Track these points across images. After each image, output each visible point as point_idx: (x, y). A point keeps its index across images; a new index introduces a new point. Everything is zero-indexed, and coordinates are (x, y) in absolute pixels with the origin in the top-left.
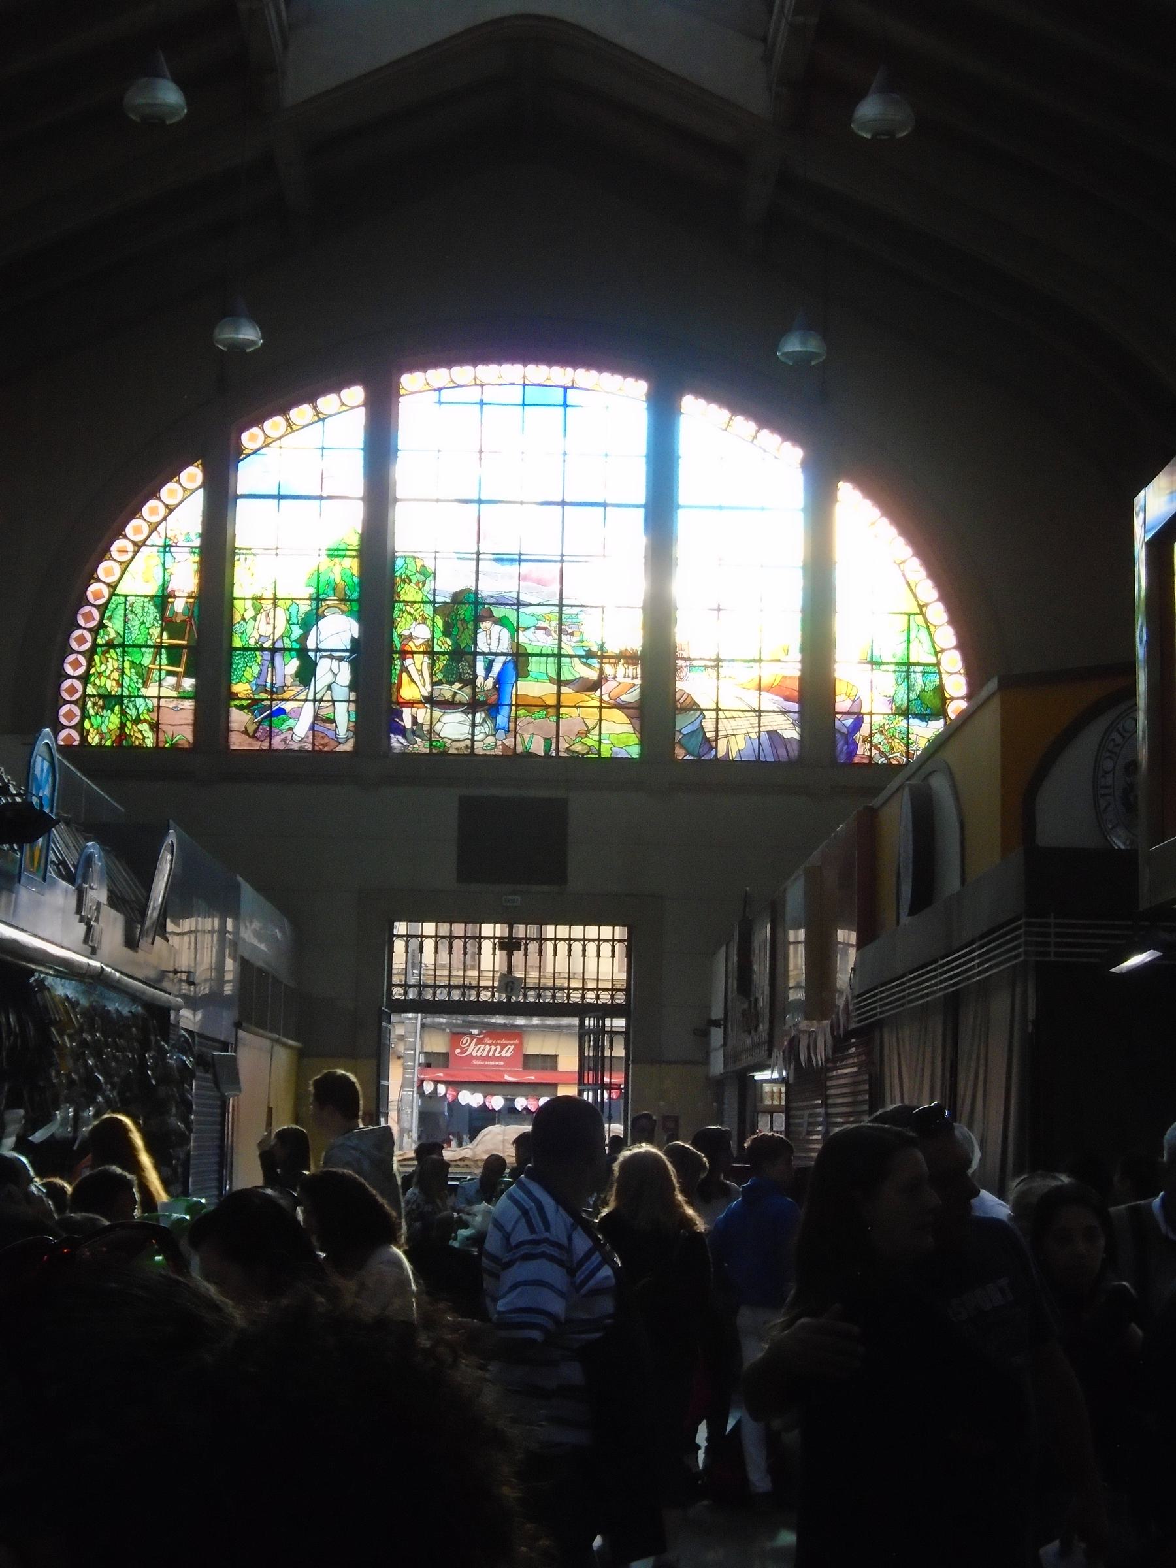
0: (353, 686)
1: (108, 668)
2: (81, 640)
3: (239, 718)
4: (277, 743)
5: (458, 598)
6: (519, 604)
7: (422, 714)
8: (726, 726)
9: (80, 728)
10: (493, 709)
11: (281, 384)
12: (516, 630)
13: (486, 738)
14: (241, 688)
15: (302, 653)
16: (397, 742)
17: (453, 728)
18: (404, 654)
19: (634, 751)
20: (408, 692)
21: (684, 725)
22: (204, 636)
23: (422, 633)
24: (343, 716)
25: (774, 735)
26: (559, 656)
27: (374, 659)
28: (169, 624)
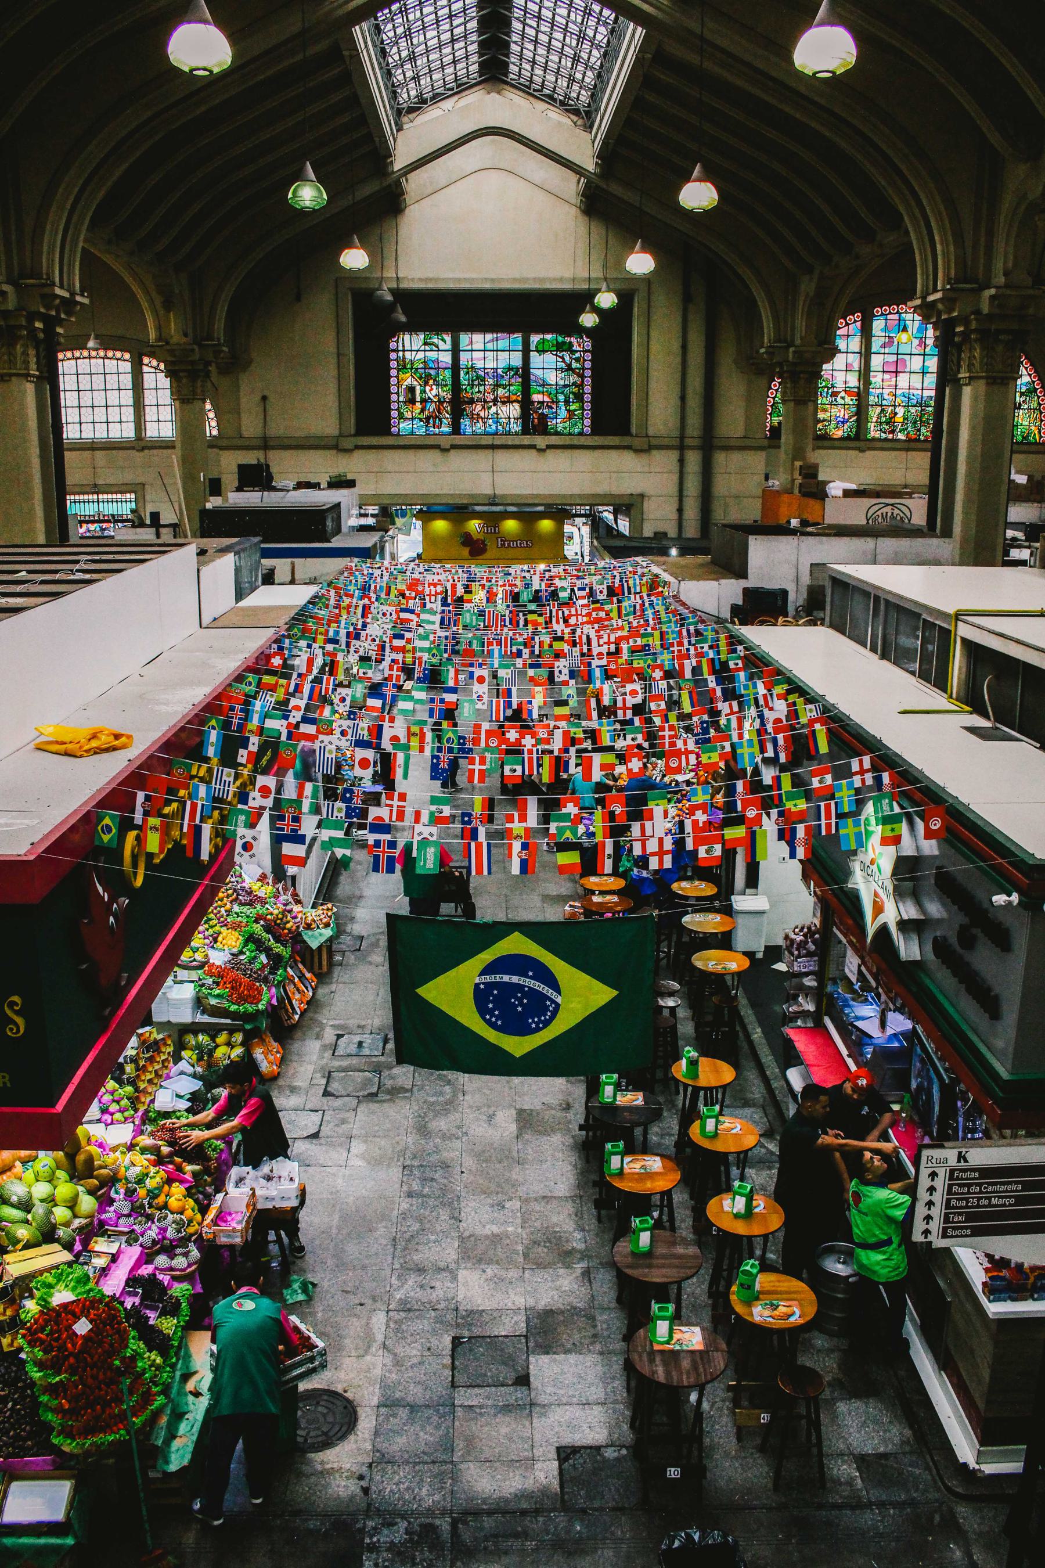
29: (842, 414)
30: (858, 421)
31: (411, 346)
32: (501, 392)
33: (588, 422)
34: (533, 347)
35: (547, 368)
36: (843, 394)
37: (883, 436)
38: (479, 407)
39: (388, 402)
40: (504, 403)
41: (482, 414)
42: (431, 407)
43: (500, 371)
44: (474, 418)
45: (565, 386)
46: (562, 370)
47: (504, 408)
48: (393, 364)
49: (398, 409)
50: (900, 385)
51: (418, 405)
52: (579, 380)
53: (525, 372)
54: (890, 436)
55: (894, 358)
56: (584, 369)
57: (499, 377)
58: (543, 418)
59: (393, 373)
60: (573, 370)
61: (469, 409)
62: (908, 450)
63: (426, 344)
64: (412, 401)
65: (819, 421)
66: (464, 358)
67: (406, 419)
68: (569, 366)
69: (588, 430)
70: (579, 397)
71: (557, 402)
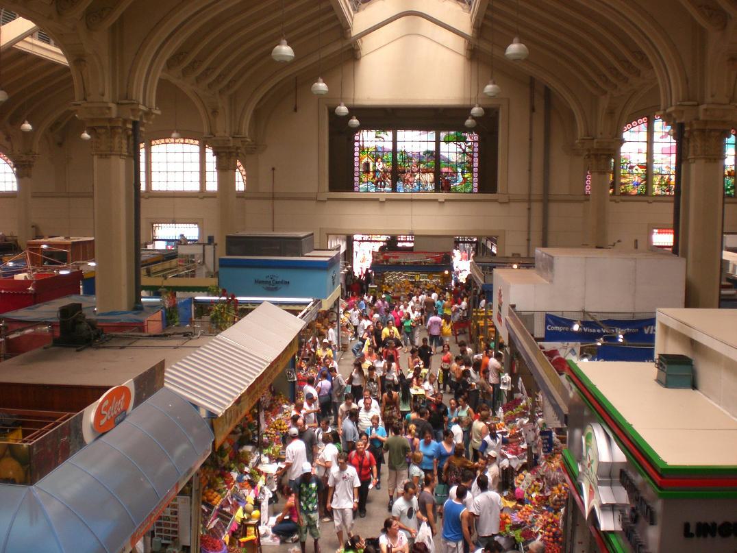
29: (637, 179)
30: (645, 184)
31: (368, 139)
32: (422, 166)
33: (476, 185)
34: (442, 139)
35: (451, 151)
36: (637, 167)
38: (408, 176)
39: (353, 172)
40: (424, 173)
41: (410, 180)
42: (379, 176)
43: (421, 154)
44: (406, 182)
45: (462, 163)
46: (460, 152)
47: (424, 176)
48: (357, 149)
49: (359, 176)
51: (371, 174)
52: (470, 159)
53: (436, 155)
54: (668, 193)
56: (473, 152)
57: (420, 157)
58: (448, 182)
59: (356, 154)
60: (467, 153)
61: (402, 176)
63: (376, 137)
64: (367, 171)
65: (622, 184)
66: (400, 147)
67: (364, 182)
68: (464, 151)
69: (476, 190)
70: (471, 170)
71: (457, 172)
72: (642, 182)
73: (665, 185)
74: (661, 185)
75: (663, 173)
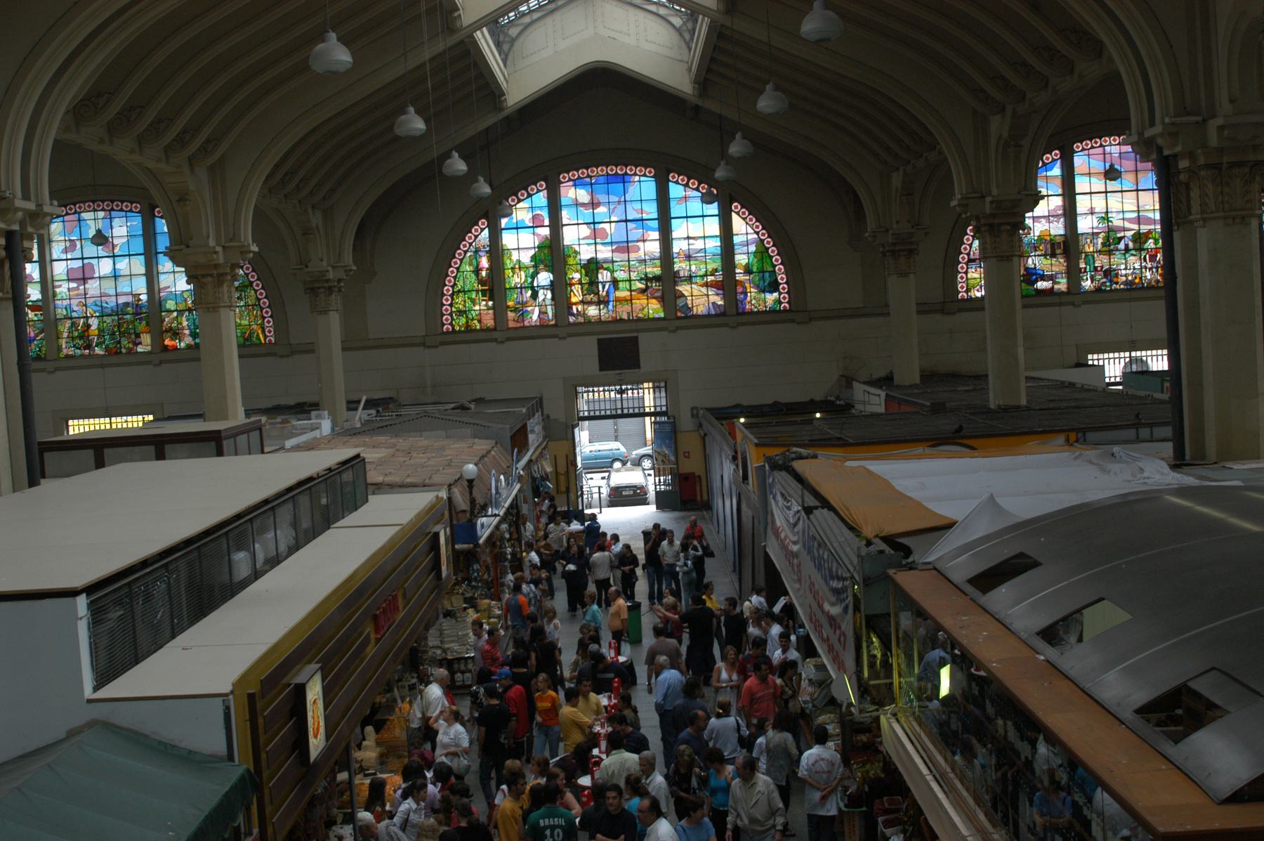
0: (553, 299)
1: (459, 299)
2: (448, 290)
3: (511, 315)
4: (526, 323)
5: (590, 261)
6: (613, 262)
7: (580, 308)
8: (696, 302)
9: (451, 324)
10: (606, 303)
11: (516, 186)
12: (612, 272)
13: (605, 313)
14: (510, 303)
15: (532, 288)
16: (571, 319)
17: (592, 311)
18: (571, 285)
19: (662, 315)
20: (574, 300)
21: (680, 302)
22: (494, 285)
23: (577, 276)
24: (550, 311)
25: (714, 303)
26: (630, 281)
27: (559, 288)
28: (481, 282)
37: (78, 352)
50: (90, 293)
55: (78, 264)
62: (102, 366)
72: (37, 335)
73: (80, 337)
74: (73, 338)
75: (74, 315)
